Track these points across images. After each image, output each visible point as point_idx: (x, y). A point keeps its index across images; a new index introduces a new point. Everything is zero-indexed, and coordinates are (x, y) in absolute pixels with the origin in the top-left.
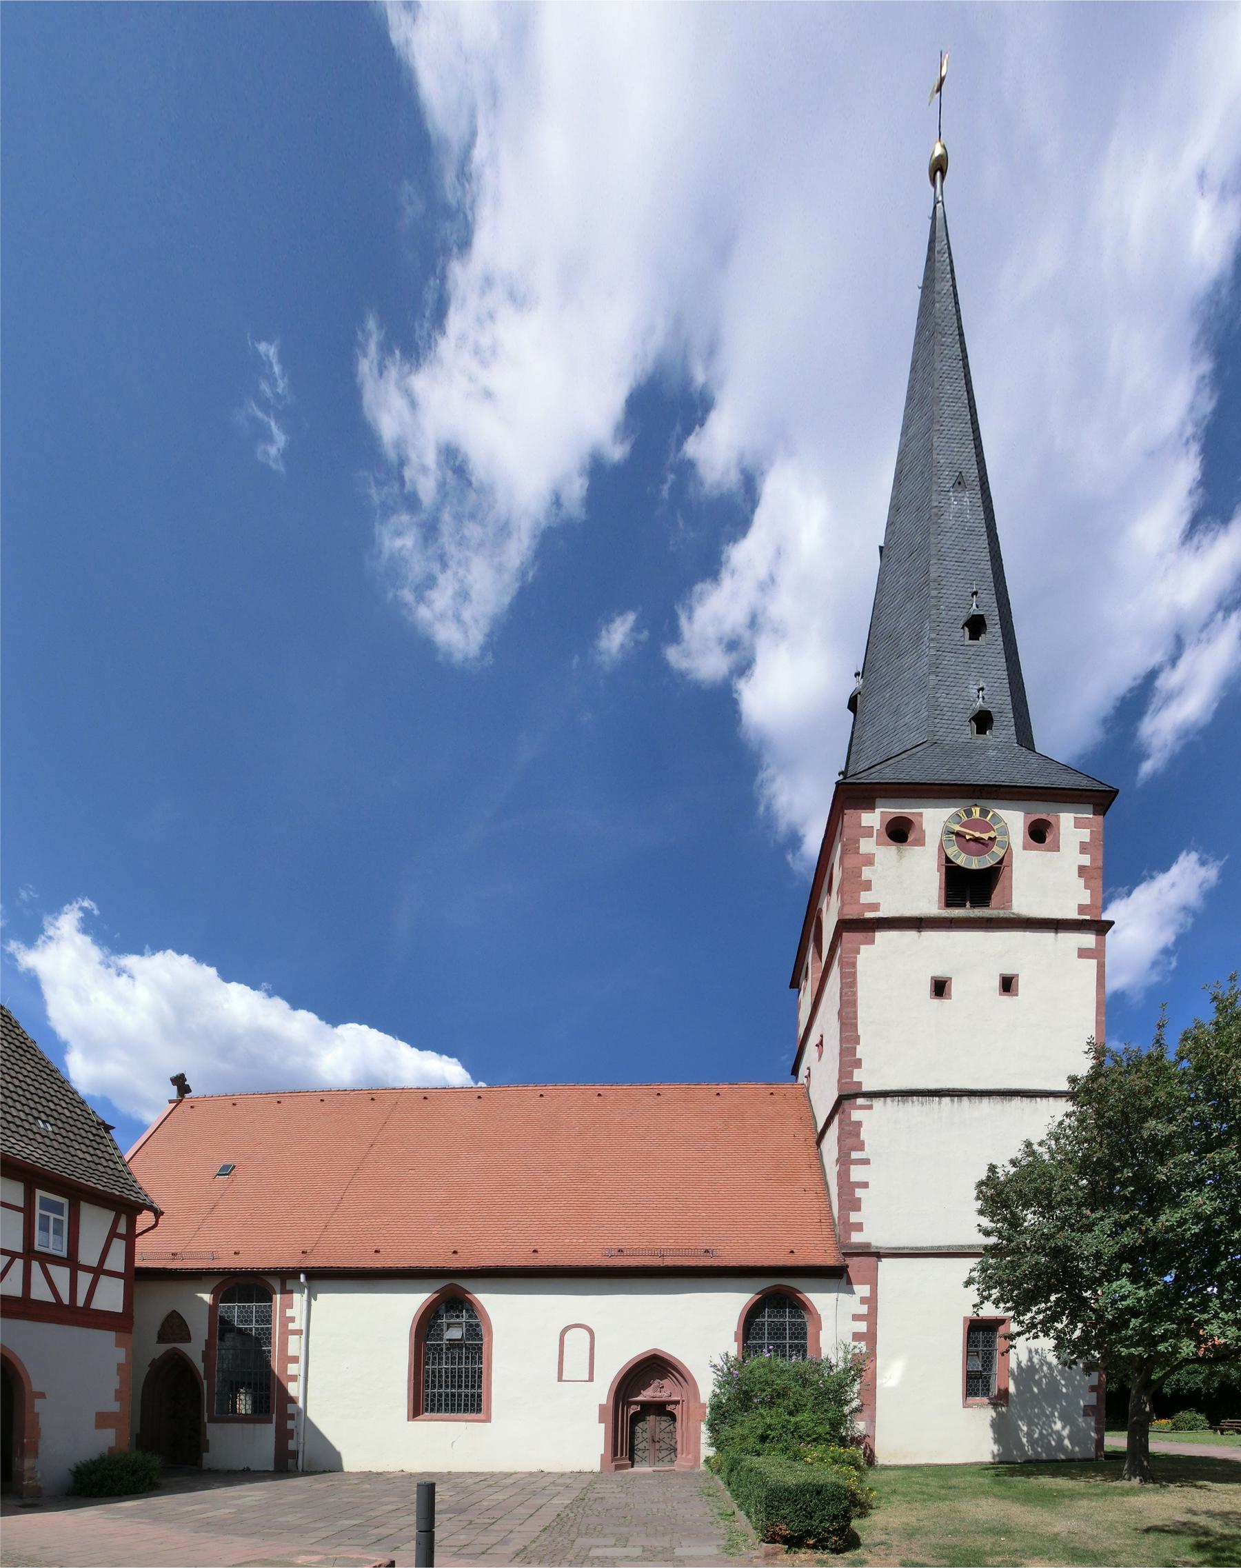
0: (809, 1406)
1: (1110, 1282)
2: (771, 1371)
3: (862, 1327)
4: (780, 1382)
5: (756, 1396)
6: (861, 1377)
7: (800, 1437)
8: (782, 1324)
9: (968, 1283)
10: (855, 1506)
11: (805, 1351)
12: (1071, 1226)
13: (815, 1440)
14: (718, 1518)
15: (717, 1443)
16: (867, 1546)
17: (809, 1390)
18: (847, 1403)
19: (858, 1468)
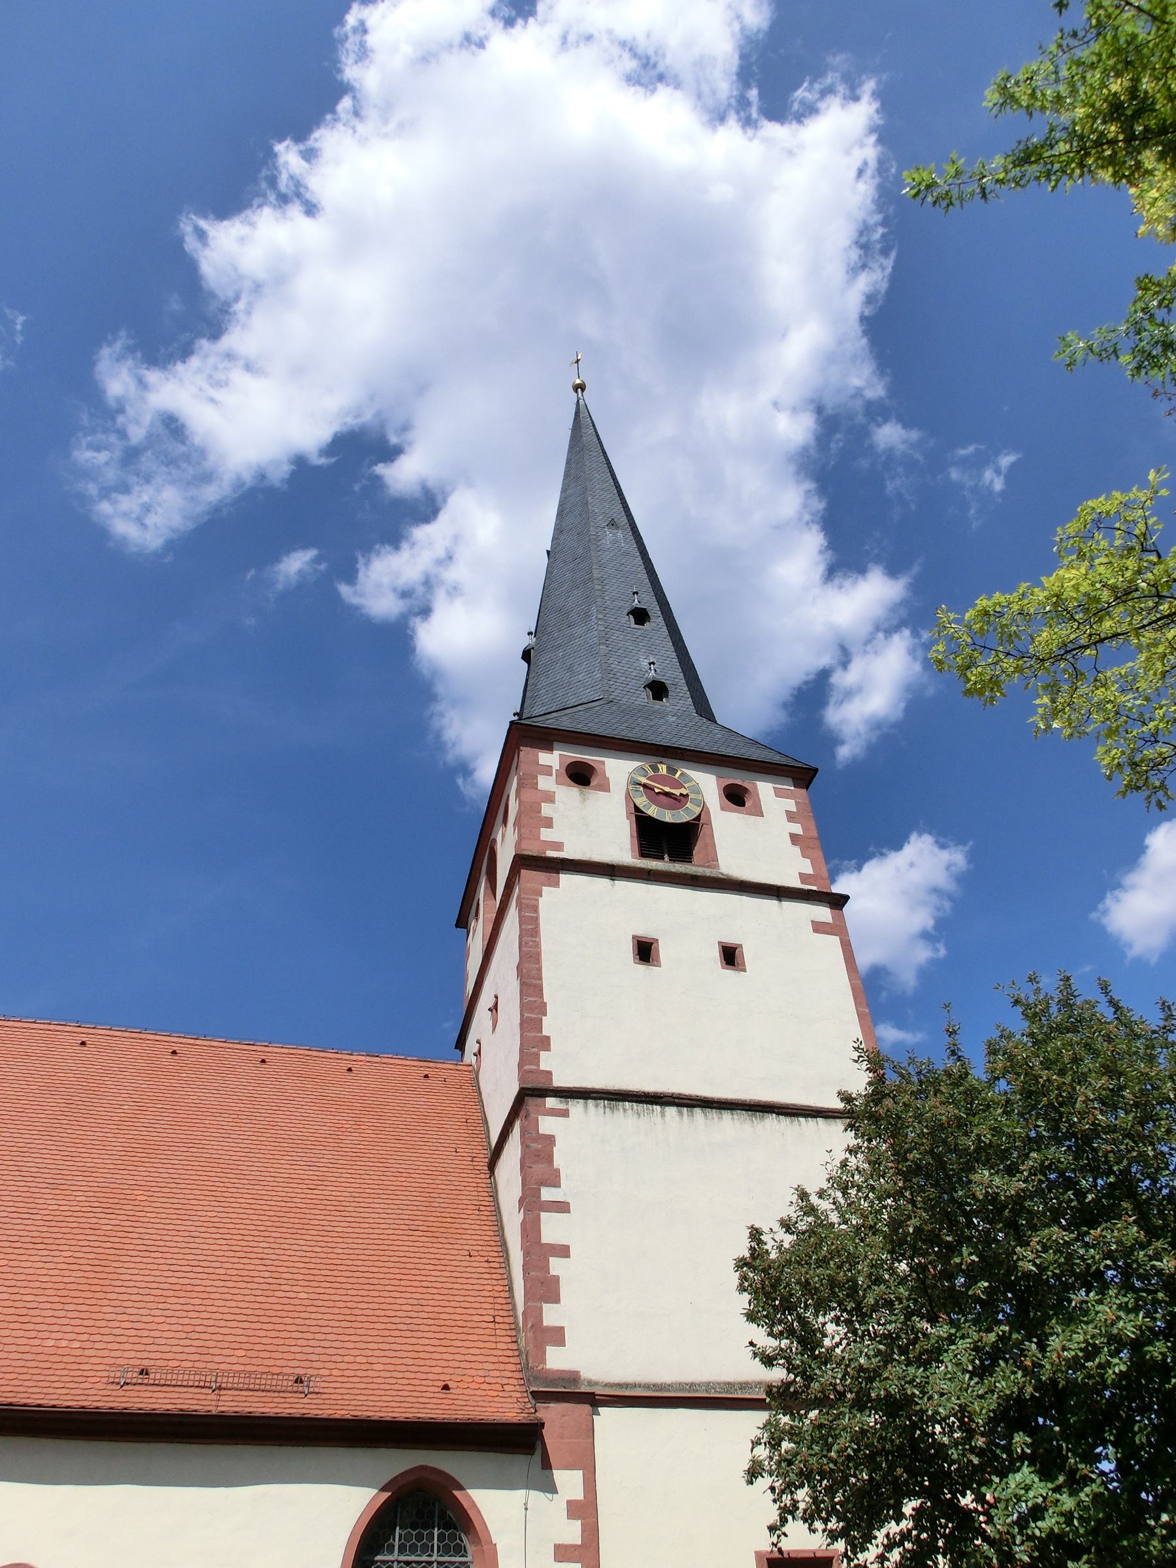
1: (1003, 1475)
9: (753, 1473)
12: (904, 1351)
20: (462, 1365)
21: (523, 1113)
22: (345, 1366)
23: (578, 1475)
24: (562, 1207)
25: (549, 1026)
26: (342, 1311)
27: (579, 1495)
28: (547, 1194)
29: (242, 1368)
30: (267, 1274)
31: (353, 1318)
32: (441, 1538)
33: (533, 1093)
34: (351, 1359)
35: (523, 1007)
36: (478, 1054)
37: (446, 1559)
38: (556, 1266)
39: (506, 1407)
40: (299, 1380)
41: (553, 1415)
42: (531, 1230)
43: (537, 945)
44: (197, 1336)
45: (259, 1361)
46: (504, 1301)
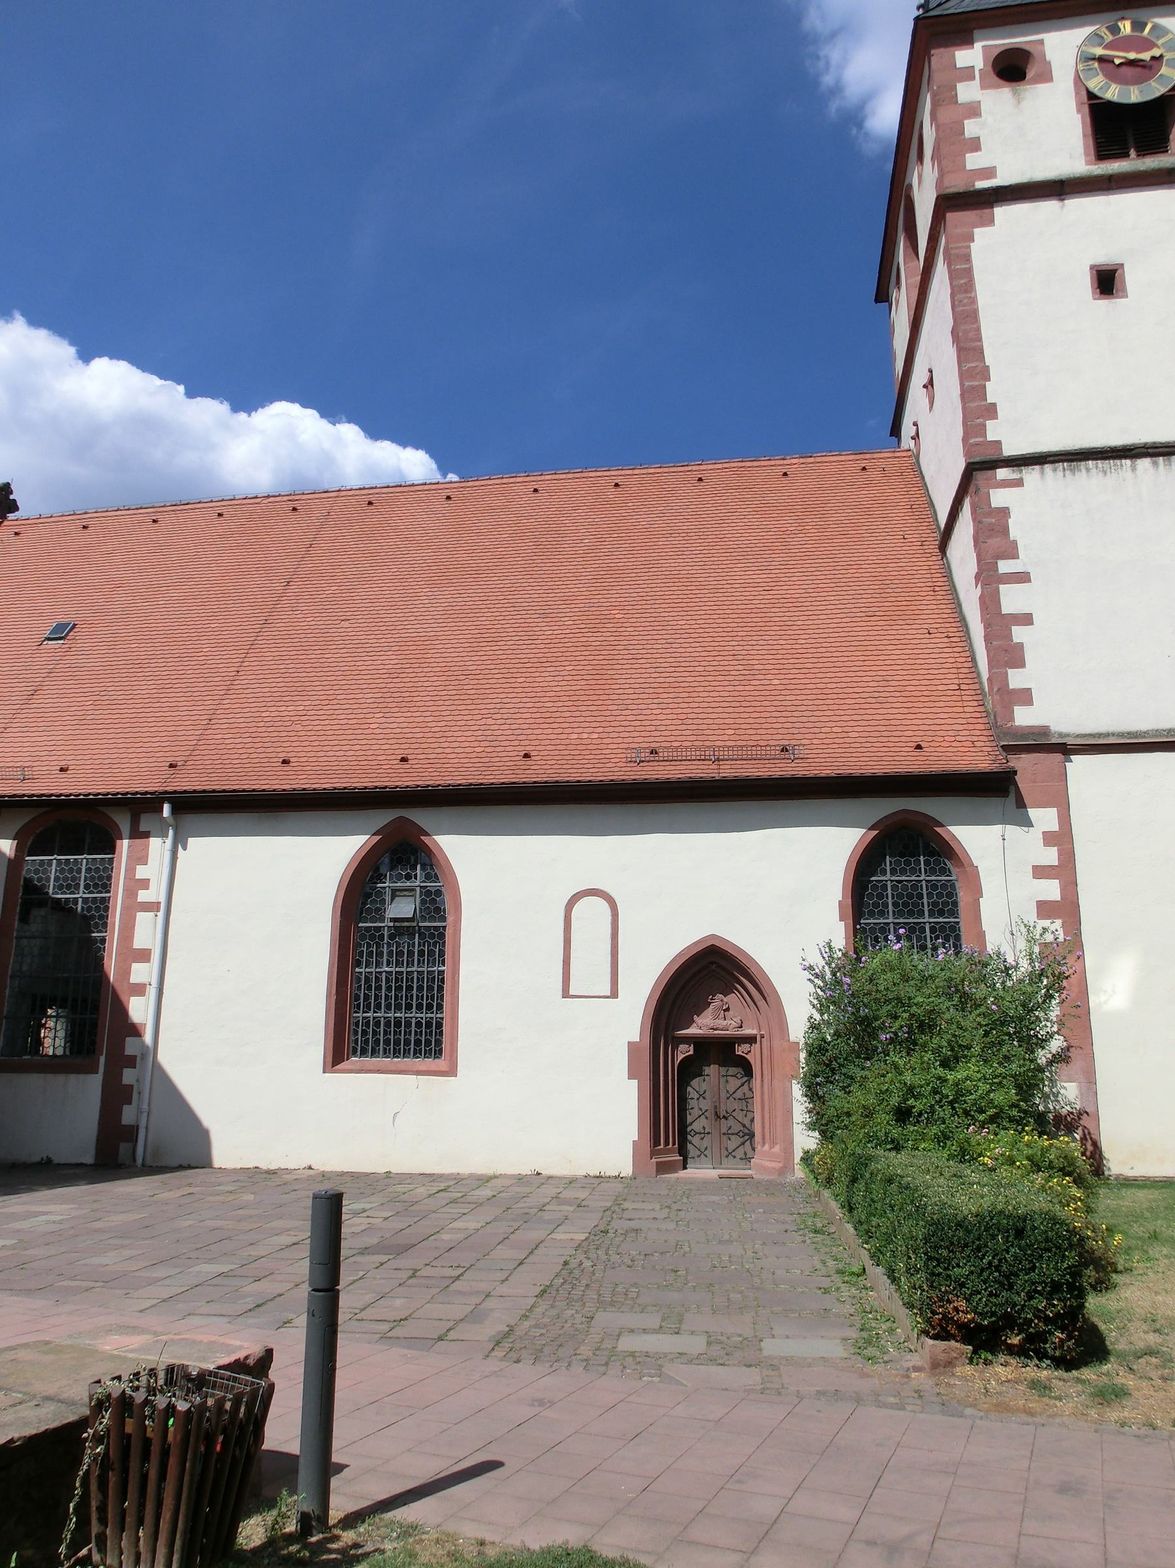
0: (976, 1049)
2: (906, 979)
3: (1051, 890)
4: (922, 1000)
5: (882, 1028)
6: (1060, 990)
7: (967, 1113)
8: (916, 885)
10: (1086, 1266)
11: (958, 938)
13: (993, 1119)
14: (837, 1279)
15: (823, 1124)
16: (1122, 1356)
17: (971, 1019)
18: (1043, 1042)
19: (1079, 1181)
20: (932, 728)
21: (972, 489)
22: (824, 736)
23: (1052, 812)
24: (1023, 578)
25: (993, 392)
26: (814, 692)
27: (1055, 827)
28: (1004, 567)
29: (733, 743)
30: (740, 667)
31: (825, 697)
32: (927, 863)
33: (981, 466)
34: (829, 730)
35: (963, 376)
36: (916, 437)
37: (933, 878)
38: (1019, 634)
39: (979, 758)
40: (784, 749)
41: (1023, 764)
42: (990, 604)
43: (974, 301)
44: (690, 721)
45: (747, 737)
46: (967, 671)
